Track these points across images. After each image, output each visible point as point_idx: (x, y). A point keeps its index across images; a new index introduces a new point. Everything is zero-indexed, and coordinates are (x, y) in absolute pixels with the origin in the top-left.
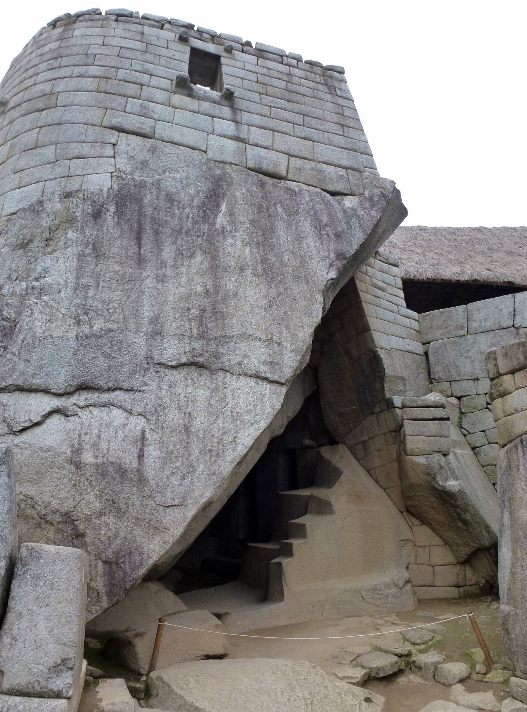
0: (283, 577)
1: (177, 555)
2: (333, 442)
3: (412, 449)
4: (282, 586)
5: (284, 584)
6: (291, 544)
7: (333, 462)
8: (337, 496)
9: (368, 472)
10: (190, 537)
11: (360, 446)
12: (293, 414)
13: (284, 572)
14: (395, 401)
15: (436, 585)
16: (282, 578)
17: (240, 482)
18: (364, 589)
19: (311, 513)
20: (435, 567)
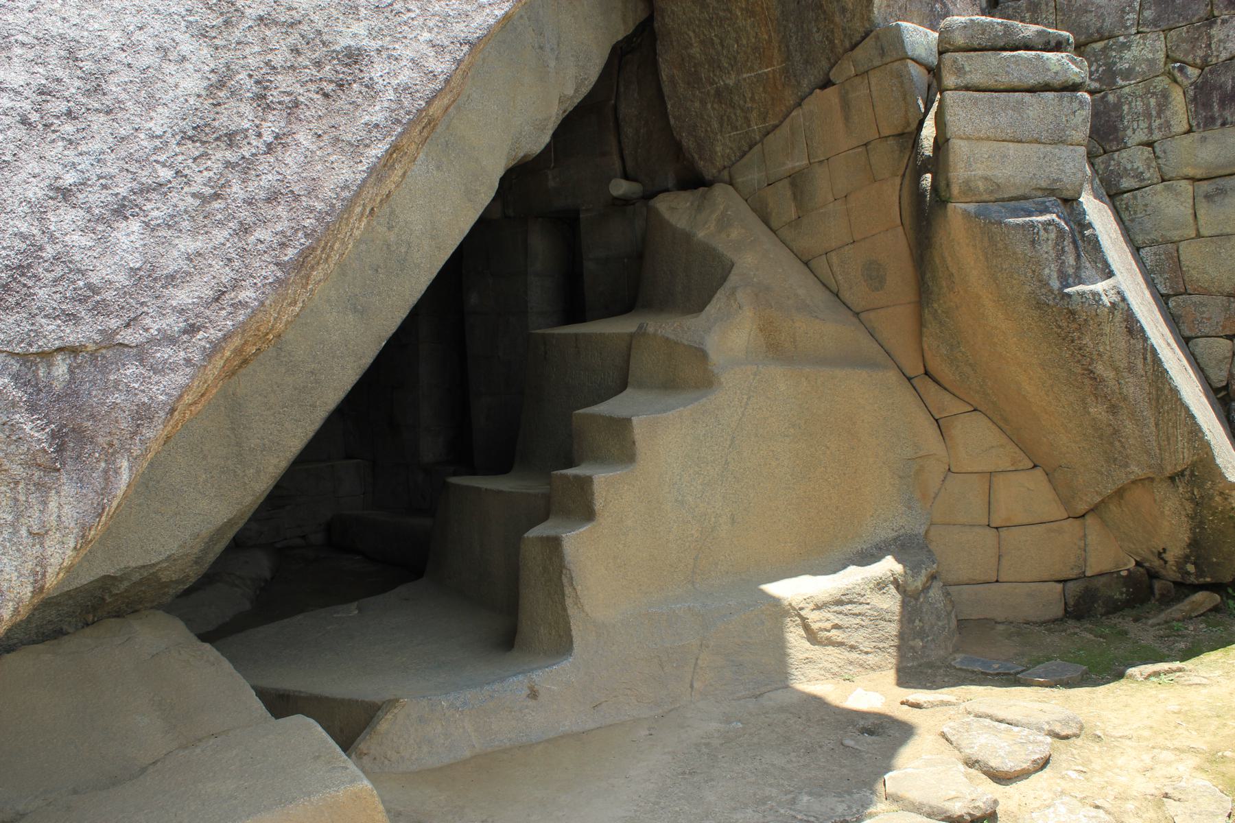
0: (565, 580)
1: (220, 531)
2: (693, 181)
3: (967, 182)
4: (565, 609)
5: (569, 602)
6: (588, 481)
7: (701, 234)
8: (728, 333)
9: (806, 264)
10: (258, 472)
11: (784, 189)
12: (576, 91)
13: (572, 567)
14: (908, 39)
15: (1002, 578)
16: (562, 586)
17: (419, 296)
18: (812, 606)
19: (641, 385)
20: (1004, 532)
